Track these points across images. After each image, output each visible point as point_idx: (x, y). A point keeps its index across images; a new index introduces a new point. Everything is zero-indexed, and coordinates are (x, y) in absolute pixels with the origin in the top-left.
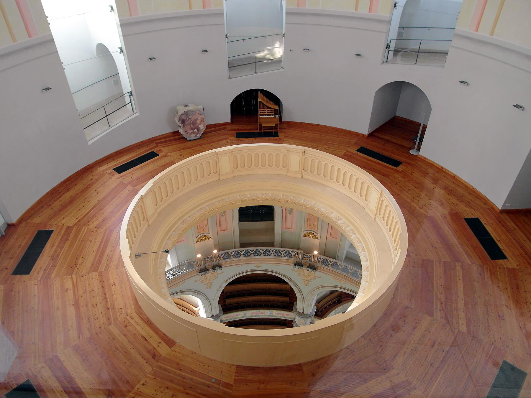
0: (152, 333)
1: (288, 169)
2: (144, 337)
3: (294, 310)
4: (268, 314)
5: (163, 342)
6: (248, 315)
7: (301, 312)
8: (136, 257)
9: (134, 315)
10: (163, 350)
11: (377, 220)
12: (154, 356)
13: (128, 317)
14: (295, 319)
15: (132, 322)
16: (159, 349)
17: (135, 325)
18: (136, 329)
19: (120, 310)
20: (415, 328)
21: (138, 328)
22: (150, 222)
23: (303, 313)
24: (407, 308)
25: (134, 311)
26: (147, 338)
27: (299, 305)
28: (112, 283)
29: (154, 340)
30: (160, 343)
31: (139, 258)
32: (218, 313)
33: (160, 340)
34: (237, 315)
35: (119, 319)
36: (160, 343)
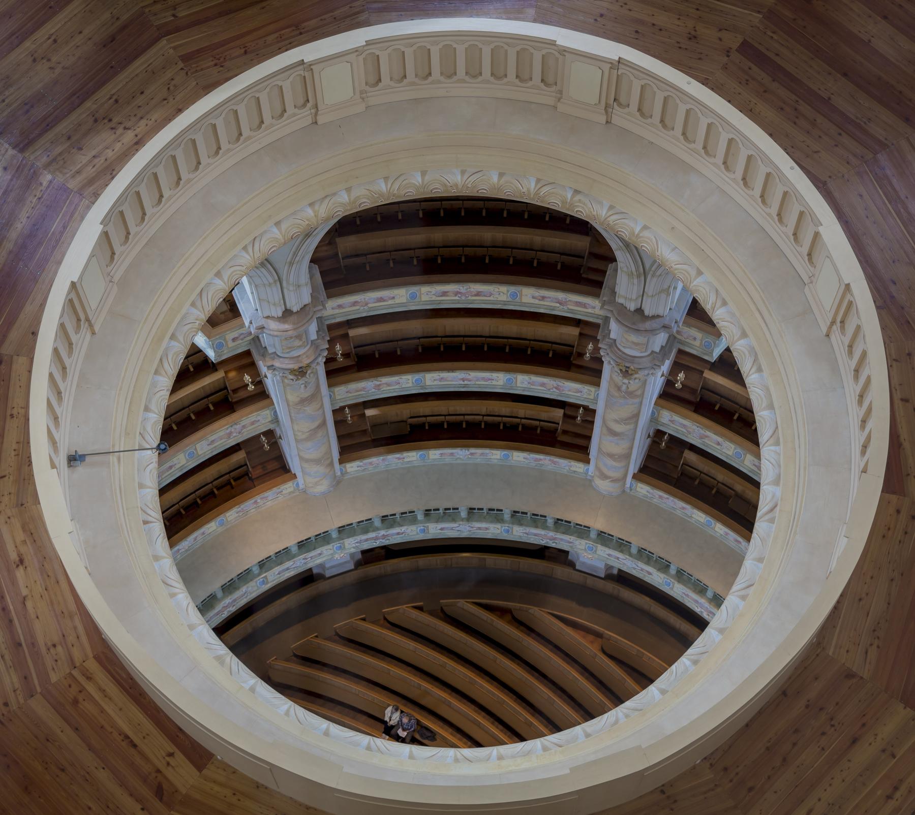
0: (148, 725)
1: (561, 92)
2: (127, 737)
3: (605, 291)
4: (503, 298)
5: (179, 756)
6: (425, 298)
7: (632, 306)
8: (70, 466)
9: (92, 666)
10: (183, 775)
11: (833, 337)
12: (159, 792)
13: (75, 673)
14: (607, 320)
15: (90, 688)
16: (169, 773)
17: (97, 696)
18: (102, 711)
19: (52, 650)
20: (855, 741)
21: (109, 709)
22: (97, 328)
23: (639, 311)
24: (850, 675)
25: (91, 655)
26: (137, 741)
27: (624, 285)
28: (13, 556)
29: (156, 746)
30: (171, 755)
31: (81, 470)
32: (307, 299)
33: (171, 748)
34: (381, 300)
35: (54, 678)
36: (171, 755)
